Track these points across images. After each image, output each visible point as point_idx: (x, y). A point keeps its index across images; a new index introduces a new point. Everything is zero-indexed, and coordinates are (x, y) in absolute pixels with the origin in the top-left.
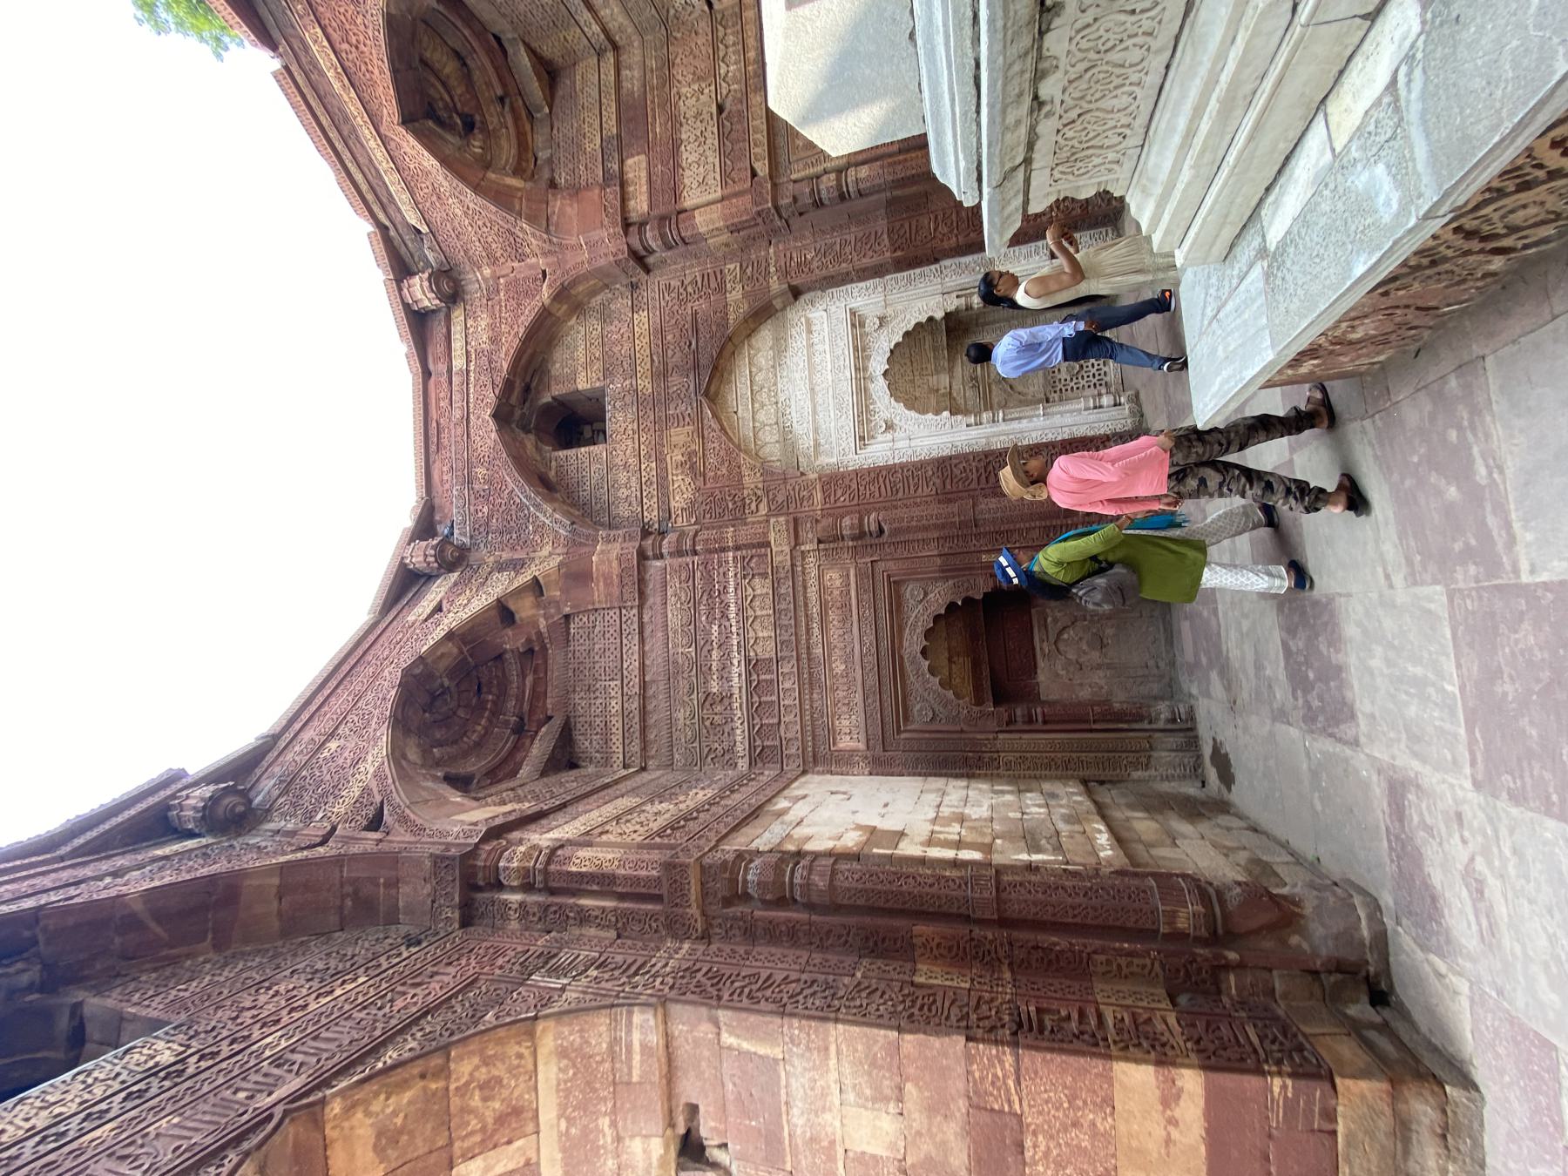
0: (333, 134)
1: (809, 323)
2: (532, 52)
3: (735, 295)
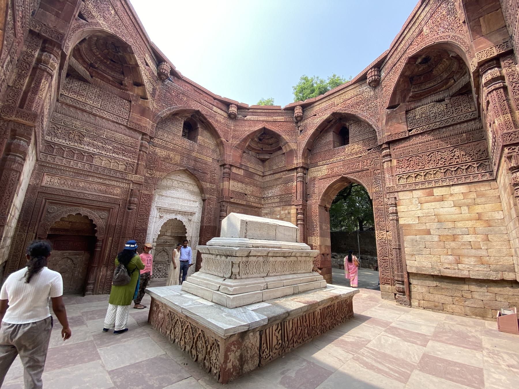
0: (267, 111)
1: (196, 202)
2: (268, 159)
3: (208, 185)
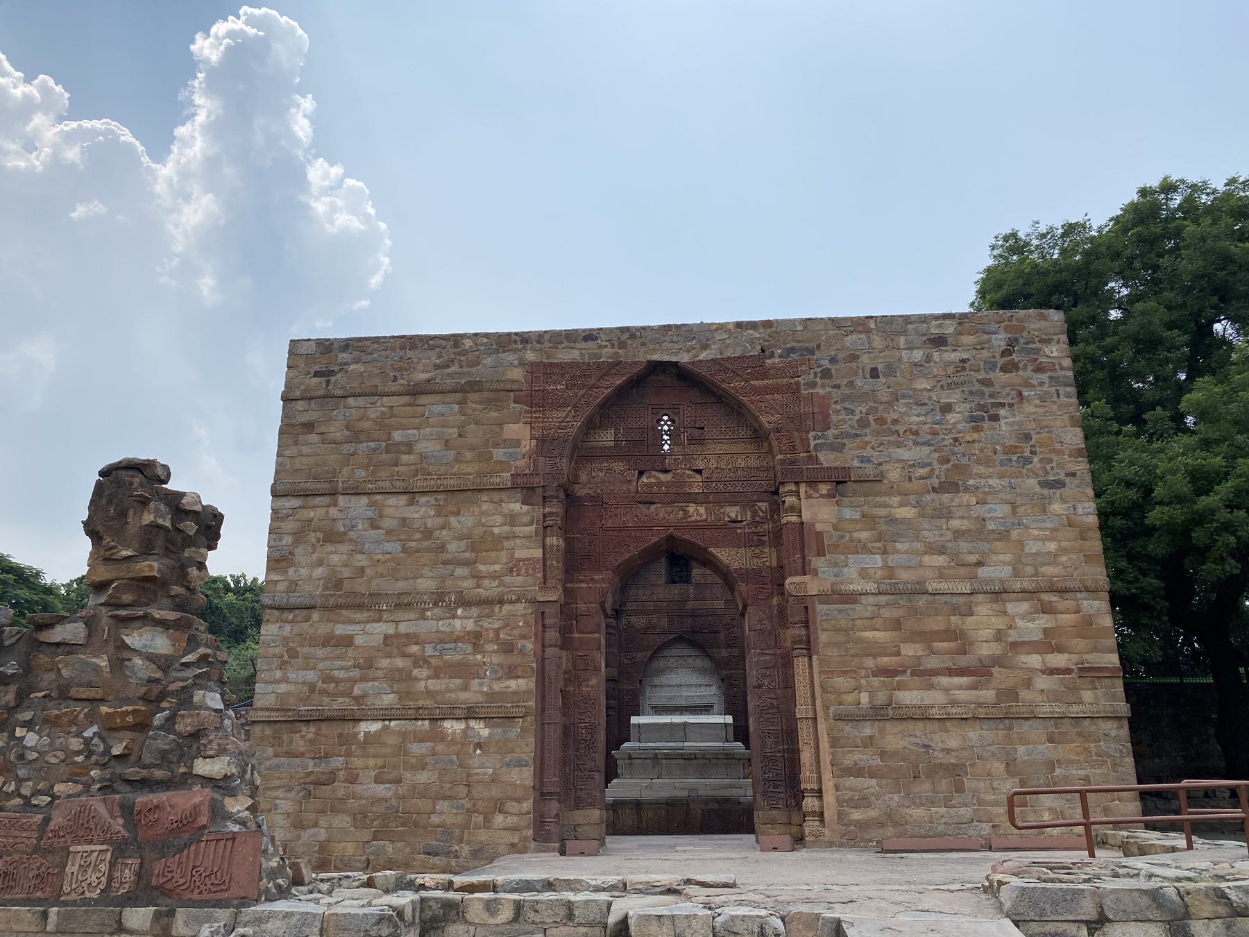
3: (724, 653)
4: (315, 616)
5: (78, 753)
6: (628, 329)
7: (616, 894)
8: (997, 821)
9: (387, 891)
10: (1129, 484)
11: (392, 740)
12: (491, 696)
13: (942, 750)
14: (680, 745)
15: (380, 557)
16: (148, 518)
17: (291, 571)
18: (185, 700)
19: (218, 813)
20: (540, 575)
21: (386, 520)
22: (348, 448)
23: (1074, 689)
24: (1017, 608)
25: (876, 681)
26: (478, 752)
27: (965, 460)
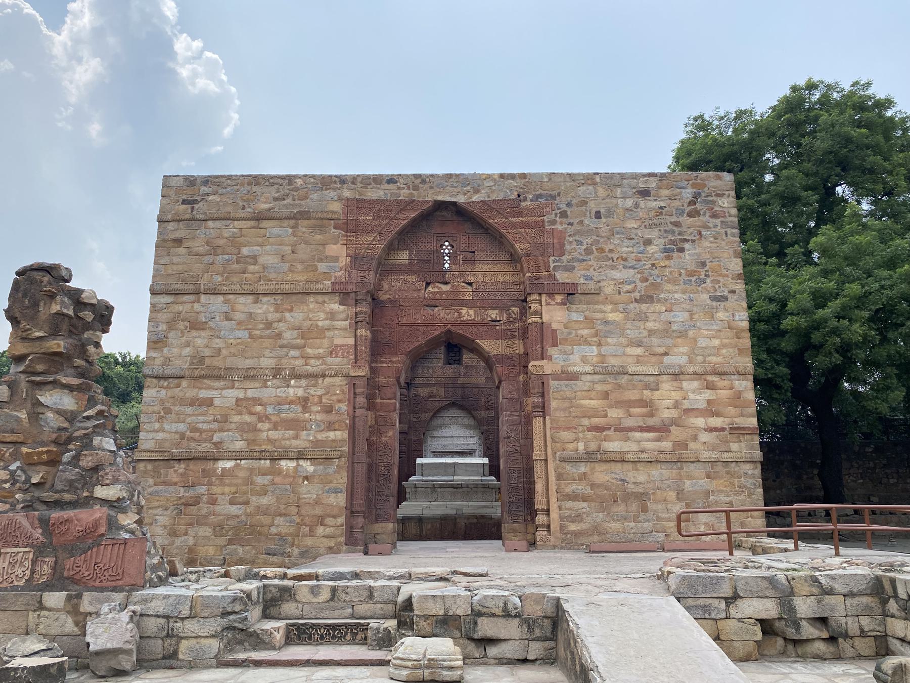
3: (484, 414)
4: (184, 383)
5: (6, 481)
6: (420, 175)
7: (404, 581)
8: (669, 531)
9: (239, 580)
10: (771, 300)
11: (242, 474)
12: (316, 443)
13: (634, 483)
14: (451, 478)
15: (232, 341)
16: (55, 308)
17: (165, 350)
18: (86, 443)
19: (113, 524)
20: (353, 357)
21: (237, 314)
22: (208, 259)
23: (725, 442)
24: (690, 385)
25: (589, 435)
26: (306, 482)
27: (659, 280)
